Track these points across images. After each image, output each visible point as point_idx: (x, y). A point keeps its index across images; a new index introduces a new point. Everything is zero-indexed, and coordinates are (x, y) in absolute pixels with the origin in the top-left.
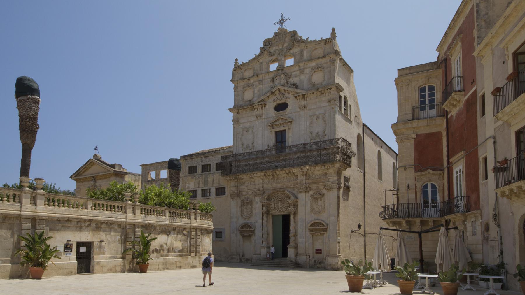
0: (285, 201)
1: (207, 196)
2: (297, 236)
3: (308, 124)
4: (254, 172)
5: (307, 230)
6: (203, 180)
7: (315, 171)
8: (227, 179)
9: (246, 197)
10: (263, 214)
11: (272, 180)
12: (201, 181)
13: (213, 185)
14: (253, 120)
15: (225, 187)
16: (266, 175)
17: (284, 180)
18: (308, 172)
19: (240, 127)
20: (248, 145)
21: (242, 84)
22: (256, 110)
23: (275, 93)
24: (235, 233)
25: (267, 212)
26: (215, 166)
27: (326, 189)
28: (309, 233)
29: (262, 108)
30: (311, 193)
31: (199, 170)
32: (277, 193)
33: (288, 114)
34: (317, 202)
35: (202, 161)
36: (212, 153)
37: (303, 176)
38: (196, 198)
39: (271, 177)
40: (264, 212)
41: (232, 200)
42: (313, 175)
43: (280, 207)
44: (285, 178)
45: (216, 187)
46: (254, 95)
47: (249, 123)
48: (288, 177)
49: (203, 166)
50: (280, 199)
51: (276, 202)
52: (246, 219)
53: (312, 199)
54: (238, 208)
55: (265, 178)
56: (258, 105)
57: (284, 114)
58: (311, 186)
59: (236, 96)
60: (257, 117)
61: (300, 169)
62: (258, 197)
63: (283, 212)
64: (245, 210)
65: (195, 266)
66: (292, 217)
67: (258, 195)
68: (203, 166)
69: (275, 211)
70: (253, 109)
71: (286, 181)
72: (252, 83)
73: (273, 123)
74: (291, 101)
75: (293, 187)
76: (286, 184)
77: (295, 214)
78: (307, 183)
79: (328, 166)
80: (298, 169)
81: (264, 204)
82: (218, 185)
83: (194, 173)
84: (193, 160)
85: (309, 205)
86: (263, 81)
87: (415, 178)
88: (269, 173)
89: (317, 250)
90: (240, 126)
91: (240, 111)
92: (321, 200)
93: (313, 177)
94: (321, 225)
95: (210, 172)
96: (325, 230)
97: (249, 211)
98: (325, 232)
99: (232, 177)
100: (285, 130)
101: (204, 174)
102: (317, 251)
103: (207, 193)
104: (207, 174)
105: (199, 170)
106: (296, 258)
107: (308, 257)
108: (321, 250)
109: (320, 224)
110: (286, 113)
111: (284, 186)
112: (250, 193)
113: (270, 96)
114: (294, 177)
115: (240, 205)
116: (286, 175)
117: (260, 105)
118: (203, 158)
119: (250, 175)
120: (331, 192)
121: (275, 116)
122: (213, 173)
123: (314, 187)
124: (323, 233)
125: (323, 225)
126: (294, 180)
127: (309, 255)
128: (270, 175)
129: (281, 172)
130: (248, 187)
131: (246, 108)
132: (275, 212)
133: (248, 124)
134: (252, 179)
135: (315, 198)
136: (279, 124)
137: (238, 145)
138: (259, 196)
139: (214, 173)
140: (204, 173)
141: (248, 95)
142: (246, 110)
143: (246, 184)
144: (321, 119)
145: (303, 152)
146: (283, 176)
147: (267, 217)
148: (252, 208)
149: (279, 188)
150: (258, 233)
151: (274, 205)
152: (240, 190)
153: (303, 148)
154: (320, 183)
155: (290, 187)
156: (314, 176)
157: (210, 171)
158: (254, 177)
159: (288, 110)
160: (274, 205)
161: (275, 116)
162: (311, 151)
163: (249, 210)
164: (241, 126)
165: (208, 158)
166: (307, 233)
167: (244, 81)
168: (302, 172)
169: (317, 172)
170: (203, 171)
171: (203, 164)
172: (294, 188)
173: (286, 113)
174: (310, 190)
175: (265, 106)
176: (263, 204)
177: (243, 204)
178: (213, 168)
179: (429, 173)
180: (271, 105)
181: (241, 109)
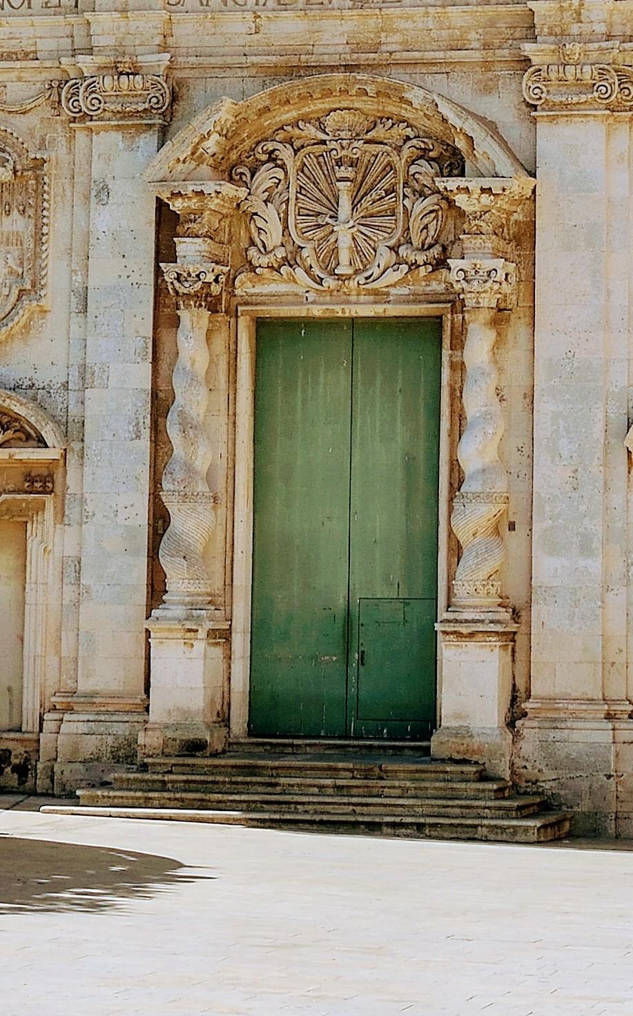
0: (391, 191)
32: (319, 106)
43: (345, 242)
50: (343, 172)
62: (116, 136)
63: (376, 293)
67: (124, 115)
75: (477, 56)
76: (403, 25)
78: (617, 30)
81: (194, 203)
111: (392, 42)
132: (283, 288)
148: (39, 237)
172: (487, 65)
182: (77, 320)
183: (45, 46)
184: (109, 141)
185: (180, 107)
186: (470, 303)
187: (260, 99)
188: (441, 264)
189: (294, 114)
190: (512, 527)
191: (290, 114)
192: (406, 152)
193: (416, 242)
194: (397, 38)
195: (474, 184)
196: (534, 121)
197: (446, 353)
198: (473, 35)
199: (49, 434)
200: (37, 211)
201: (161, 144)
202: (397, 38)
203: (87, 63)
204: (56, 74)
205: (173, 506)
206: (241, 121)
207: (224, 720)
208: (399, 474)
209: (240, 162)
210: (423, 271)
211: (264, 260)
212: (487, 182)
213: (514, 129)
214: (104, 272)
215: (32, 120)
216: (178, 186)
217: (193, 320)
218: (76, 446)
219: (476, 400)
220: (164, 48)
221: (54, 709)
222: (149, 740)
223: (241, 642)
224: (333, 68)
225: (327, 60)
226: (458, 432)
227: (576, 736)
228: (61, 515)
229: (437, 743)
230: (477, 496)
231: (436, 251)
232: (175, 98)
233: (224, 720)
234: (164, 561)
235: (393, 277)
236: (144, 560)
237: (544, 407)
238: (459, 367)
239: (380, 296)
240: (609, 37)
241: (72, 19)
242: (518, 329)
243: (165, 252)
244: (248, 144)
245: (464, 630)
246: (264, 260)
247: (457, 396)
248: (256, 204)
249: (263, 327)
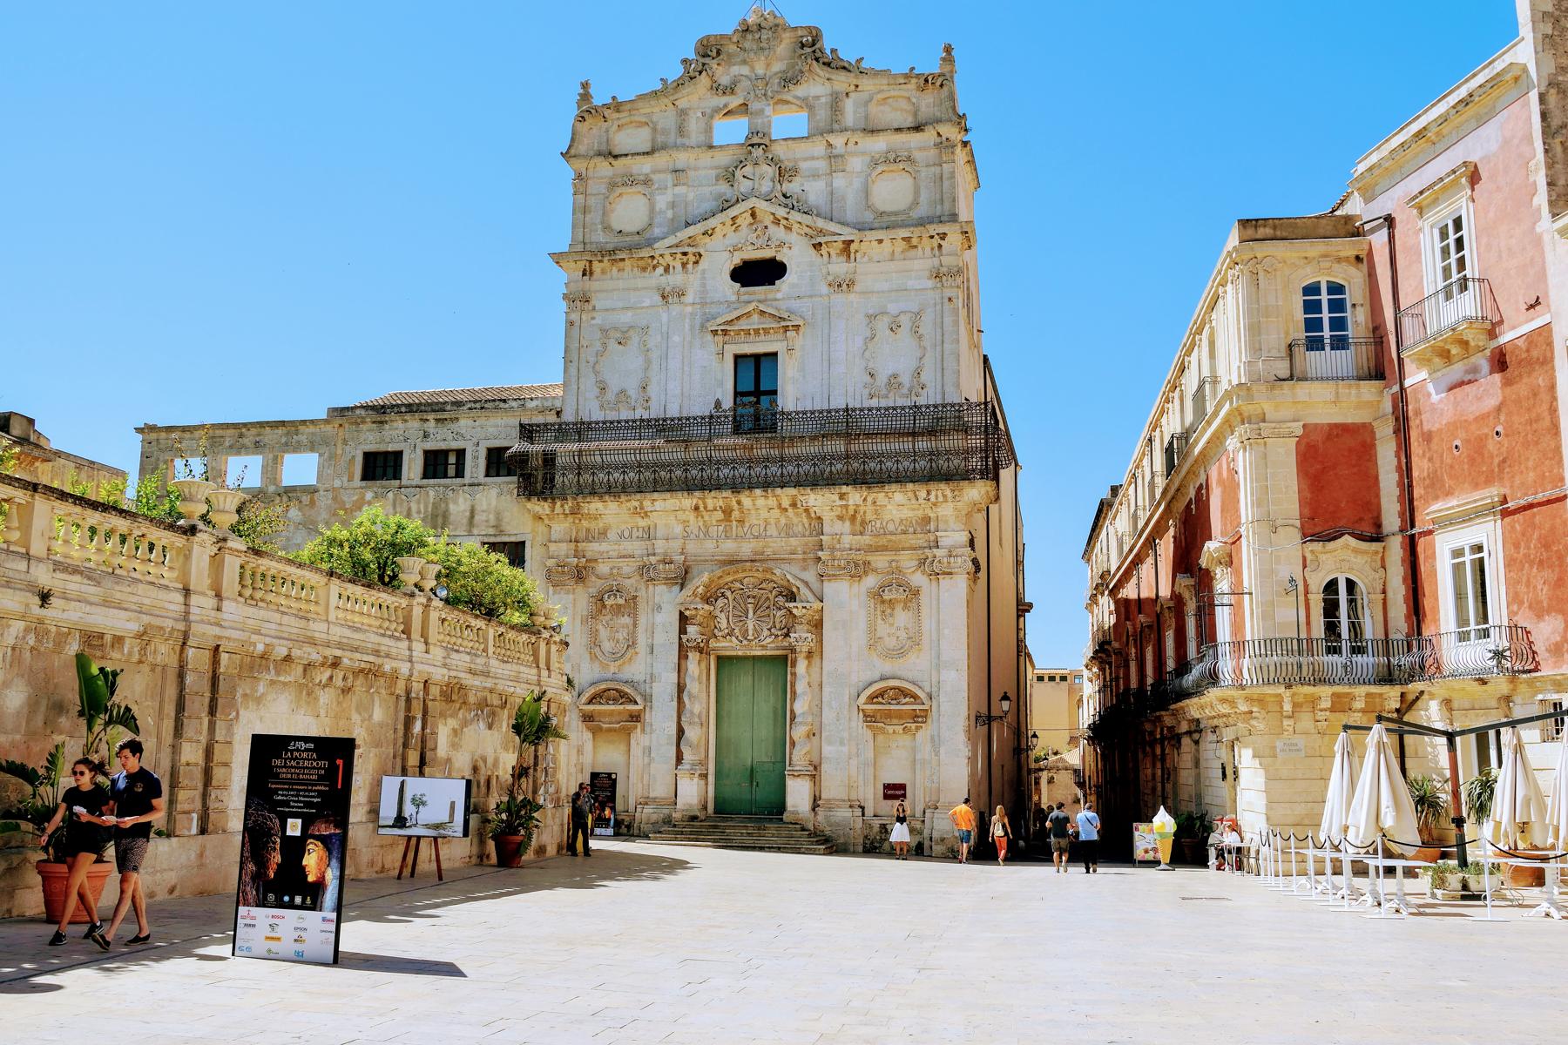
3: (859, 341)
4: (656, 495)
6: (426, 507)
7: (889, 507)
8: (541, 512)
9: (615, 583)
12: (419, 512)
13: (470, 531)
14: (644, 305)
15: (524, 543)
16: (702, 509)
17: (765, 530)
18: (862, 509)
19: (593, 322)
20: (623, 391)
21: (603, 168)
22: (660, 270)
23: (738, 221)
26: (482, 462)
27: (924, 572)
28: (861, 723)
29: (684, 265)
30: (871, 581)
31: (412, 467)
32: (741, 575)
33: (784, 299)
34: (891, 615)
35: (426, 435)
36: (470, 409)
39: (719, 515)
41: (554, 593)
43: (751, 627)
44: (772, 521)
46: (651, 218)
47: (630, 313)
48: (783, 521)
49: (426, 453)
50: (750, 600)
54: (578, 622)
55: (691, 516)
56: (672, 254)
57: (770, 296)
58: (869, 558)
59: (582, 210)
60: (664, 297)
61: (836, 497)
62: (664, 587)
63: (763, 646)
64: (604, 633)
66: (801, 667)
67: (667, 579)
68: (426, 453)
70: (650, 265)
71: (775, 533)
72: (647, 174)
73: (730, 322)
74: (796, 255)
75: (801, 556)
76: (771, 544)
79: (939, 493)
80: (828, 495)
81: (693, 612)
82: (491, 531)
83: (384, 476)
84: (387, 427)
86: (691, 174)
87: (1304, 559)
88: (715, 500)
89: (887, 787)
90: (593, 318)
91: (597, 266)
92: (906, 608)
93: (878, 525)
94: (907, 699)
95: (459, 480)
96: (920, 717)
97: (621, 638)
99: (562, 506)
100: (775, 354)
101: (434, 486)
102: (889, 792)
104: (446, 487)
105: (412, 467)
106: (816, 814)
107: (858, 812)
108: (902, 787)
109: (904, 693)
110: (779, 296)
111: (769, 551)
114: (805, 520)
115: (585, 613)
116: (776, 512)
117: (679, 256)
118: (432, 423)
119: (637, 504)
120: (945, 582)
121: (734, 298)
122: (470, 485)
123: (880, 561)
124: (913, 726)
125: (915, 697)
126: (807, 533)
128: (716, 510)
129: (761, 502)
130: (621, 547)
131: (623, 260)
132: (727, 644)
133: (626, 318)
134: (639, 519)
135: (883, 602)
136: (752, 332)
137: (582, 387)
138: (670, 582)
139: (479, 485)
140: (432, 481)
141: (629, 212)
142: (621, 264)
143: (612, 535)
144: (904, 331)
145: (848, 436)
146: (764, 513)
148: (635, 625)
149: (746, 558)
150: (661, 719)
152: (589, 555)
153: (846, 424)
157: (460, 473)
159: (784, 285)
161: (734, 298)
162: (868, 435)
164: (598, 321)
165: (454, 426)
166: (854, 724)
167: (613, 162)
168: (841, 506)
169: (894, 512)
170: (425, 476)
171: (431, 445)
173: (779, 296)
174: (866, 573)
175: (696, 263)
178: (476, 465)
179: (1347, 546)
180: (720, 261)
181: (600, 261)
182: (649, 656)
183: (637, 553)
184: (661, 589)
185: (688, 576)
186: (798, 650)
187: (719, 573)
188: (787, 635)
189: (731, 579)
190: (814, 735)
191: (729, 578)
192: (774, 593)
193: (778, 627)
194: (771, 550)
195: (800, 605)
196: (822, 581)
197: (789, 669)
199: (639, 699)
200: (634, 616)
201: (681, 590)
202: (771, 550)
203: (653, 559)
204: (641, 563)
205: (685, 728)
206: (711, 581)
207: (705, 808)
208: (771, 715)
209: (711, 597)
210: (780, 638)
211: (720, 634)
212: (804, 604)
213: (815, 585)
214: (659, 639)
215: (632, 581)
216: (687, 606)
217: (693, 657)
218: (649, 704)
219: (801, 687)
220: (682, 553)
221: (640, 804)
222: (677, 815)
223: (711, 779)
224: (746, 561)
225: (744, 558)
226: (793, 699)
227: (838, 814)
228: (643, 730)
229: (785, 817)
230: (801, 723)
231: (785, 630)
232: (686, 572)
233: (705, 808)
234: (682, 747)
235: (768, 640)
236: (674, 748)
237: (826, 689)
238: (794, 674)
239: (764, 647)
240: (851, 549)
241: (647, 542)
242: (816, 659)
243: (683, 631)
244: (713, 590)
245: (796, 774)
246: (720, 634)
247: (793, 685)
248: (717, 613)
249: (720, 659)
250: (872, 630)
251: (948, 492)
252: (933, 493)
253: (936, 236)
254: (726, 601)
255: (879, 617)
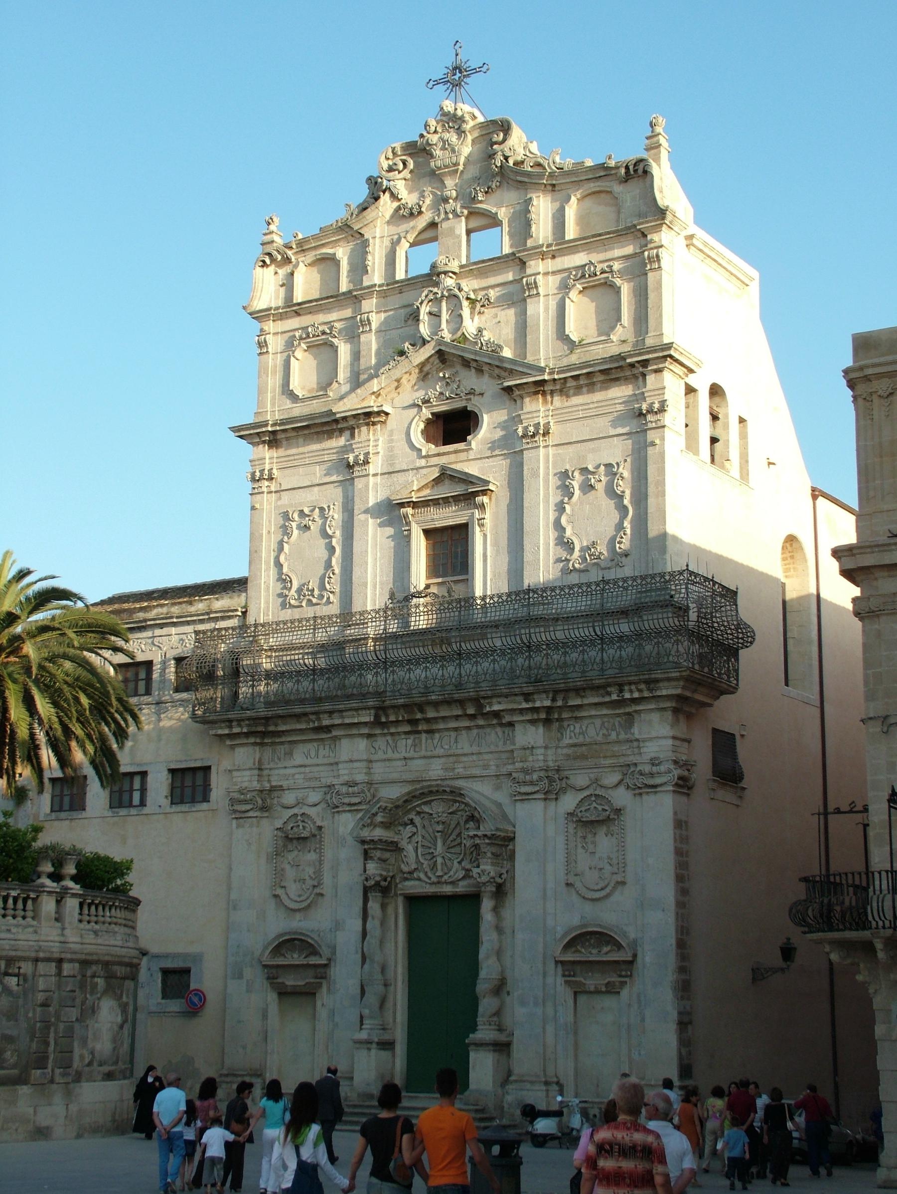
1: (131, 805)
2: (508, 993)
5: (551, 965)
10: (366, 890)
11: (410, 742)
15: (209, 768)
17: (456, 741)
24: (248, 973)
25: (383, 884)
27: (628, 787)
28: (560, 980)
30: (569, 802)
34: (594, 843)
37: (537, 729)
38: (84, 814)
40: (368, 884)
41: (238, 827)
42: (578, 726)
43: (439, 860)
45: (173, 766)
51: (423, 837)
52: (294, 911)
53: (571, 831)
62: (349, 815)
64: (290, 873)
65: (48, 1128)
66: (487, 905)
67: (350, 804)
69: (419, 879)
77: (501, 891)
85: (561, 857)
93: (577, 731)
94: (609, 948)
98: (626, 976)
103: (131, 790)
112: (314, 797)
113: (404, 381)
117: (362, 417)
120: (649, 800)
125: (619, 946)
127: (558, 1083)
136: (441, 501)
147: (384, 907)
148: (321, 862)
151: (416, 852)
154: (605, 757)
155: (485, 773)
156: (581, 727)
158: (333, 726)
160: (416, 852)
163: (310, 871)
166: (550, 980)
174: (563, 790)
176: (366, 847)
177: (285, 846)
194: (461, 765)
198: (492, 763)
200: (320, 851)
215: (319, 808)
223: (401, 1049)
248: (403, 844)
250: (570, 862)
251: (642, 686)
252: (626, 688)
253: (637, 365)
254: (414, 830)
255: (580, 845)
